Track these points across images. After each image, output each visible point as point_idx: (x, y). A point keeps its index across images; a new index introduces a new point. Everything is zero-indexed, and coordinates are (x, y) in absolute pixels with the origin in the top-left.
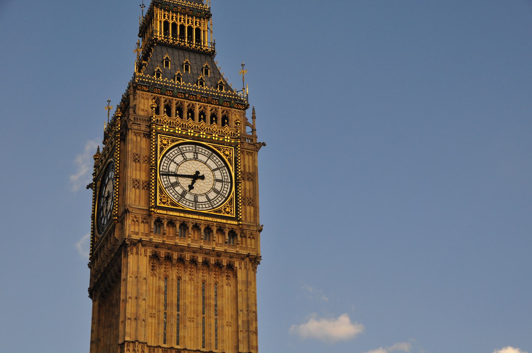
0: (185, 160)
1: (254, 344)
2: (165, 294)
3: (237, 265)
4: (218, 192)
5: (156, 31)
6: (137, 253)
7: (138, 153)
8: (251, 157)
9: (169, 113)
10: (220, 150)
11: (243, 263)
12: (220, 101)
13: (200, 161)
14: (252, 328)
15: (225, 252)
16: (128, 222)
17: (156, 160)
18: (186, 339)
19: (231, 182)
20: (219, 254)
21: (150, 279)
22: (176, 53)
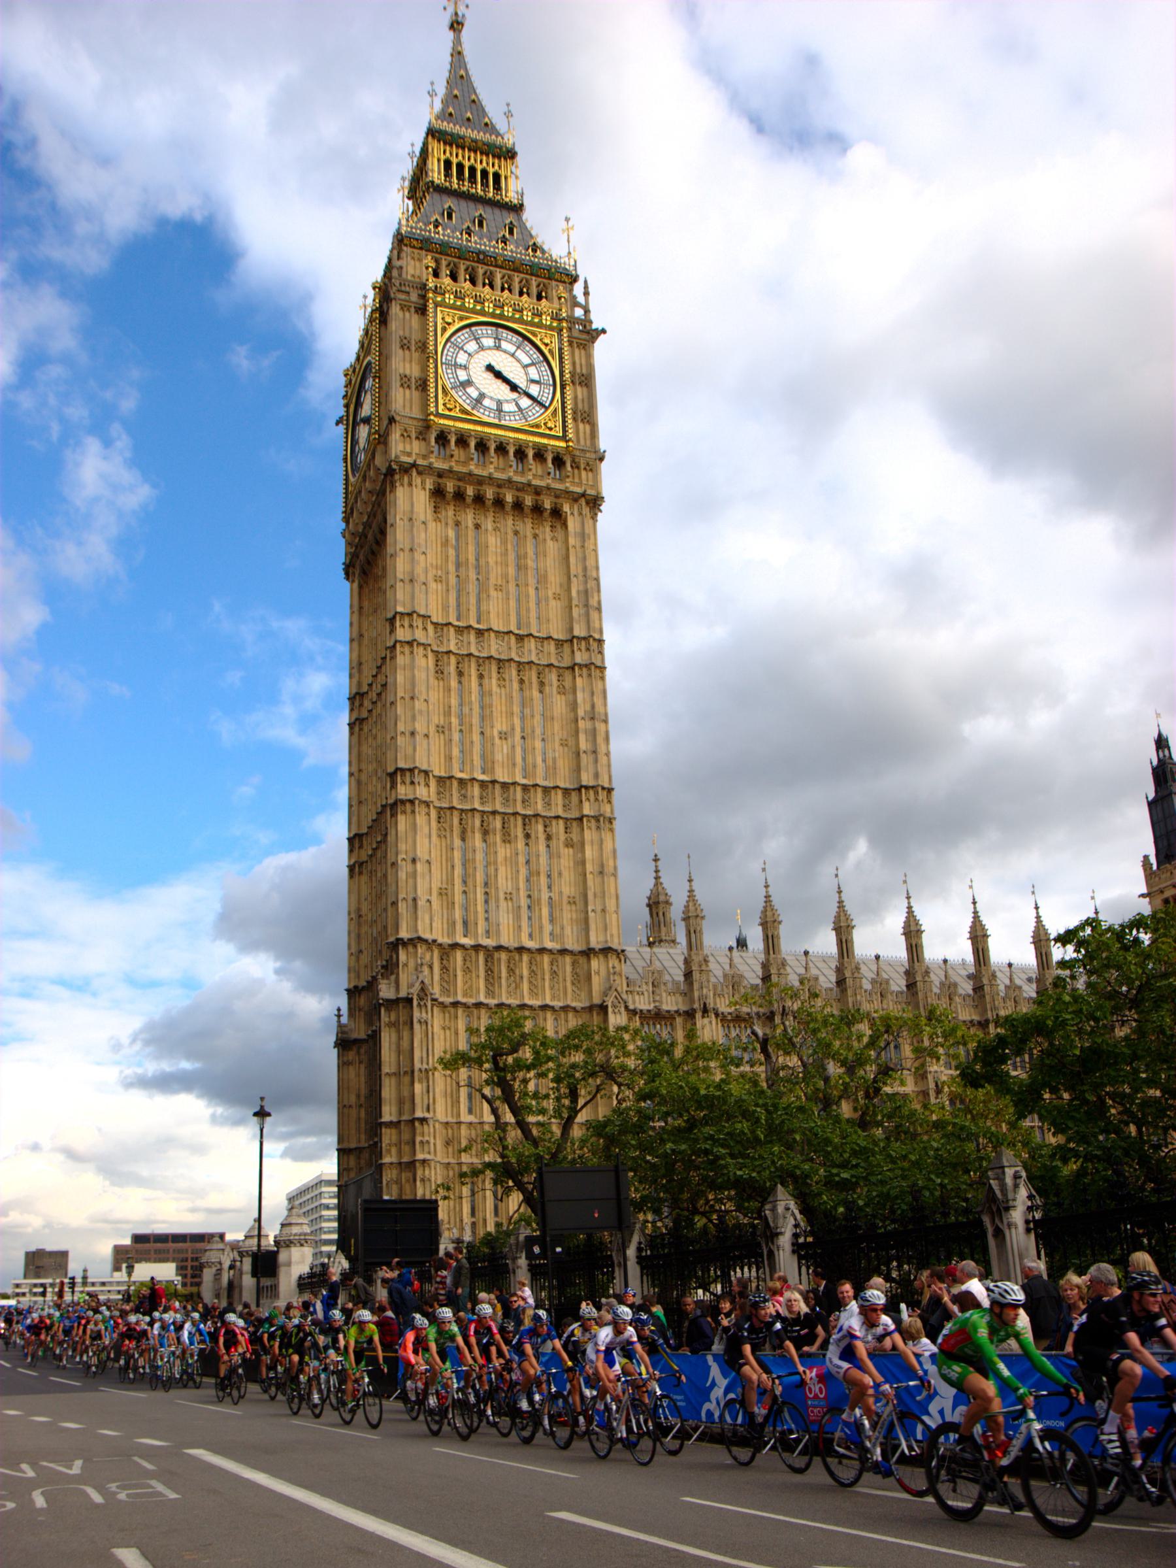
0: (482, 348)
1: (597, 625)
2: (457, 549)
3: (566, 508)
5: (433, 171)
6: (410, 485)
7: (407, 335)
8: (583, 352)
10: (535, 335)
11: (576, 507)
12: (534, 270)
13: (505, 352)
14: (593, 602)
15: (548, 488)
18: (492, 616)
20: (537, 491)
22: (463, 203)
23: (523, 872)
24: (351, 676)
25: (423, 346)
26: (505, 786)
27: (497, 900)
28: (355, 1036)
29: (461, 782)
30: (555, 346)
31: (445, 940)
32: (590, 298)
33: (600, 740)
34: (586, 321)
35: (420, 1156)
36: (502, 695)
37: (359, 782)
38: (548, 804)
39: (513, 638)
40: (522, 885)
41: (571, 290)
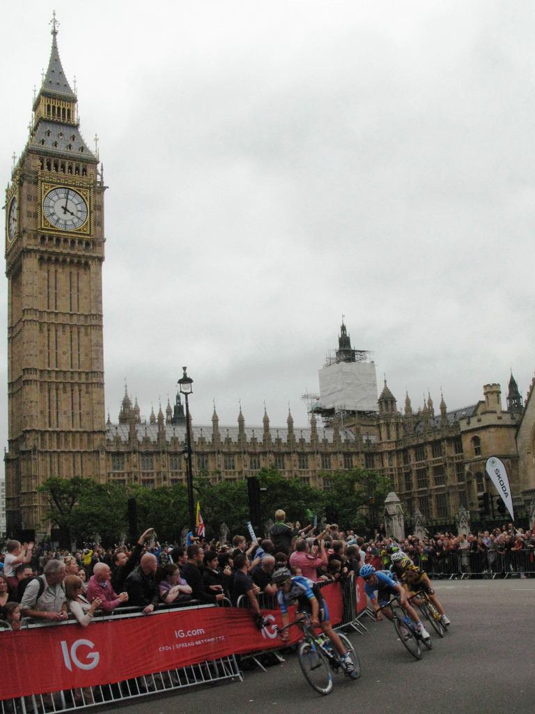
0: (59, 198)
4: (79, 219)
9: (49, 169)
16: (25, 238)
19: (87, 212)
20: (80, 256)
24: (9, 319)
25: (36, 199)
26: (65, 372)
27: (61, 414)
28: (11, 457)
29: (49, 371)
30: (88, 195)
31: (43, 429)
32: (104, 172)
33: (100, 354)
34: (101, 183)
36: (64, 338)
37: (12, 362)
38: (80, 378)
40: (70, 408)
41: (96, 167)
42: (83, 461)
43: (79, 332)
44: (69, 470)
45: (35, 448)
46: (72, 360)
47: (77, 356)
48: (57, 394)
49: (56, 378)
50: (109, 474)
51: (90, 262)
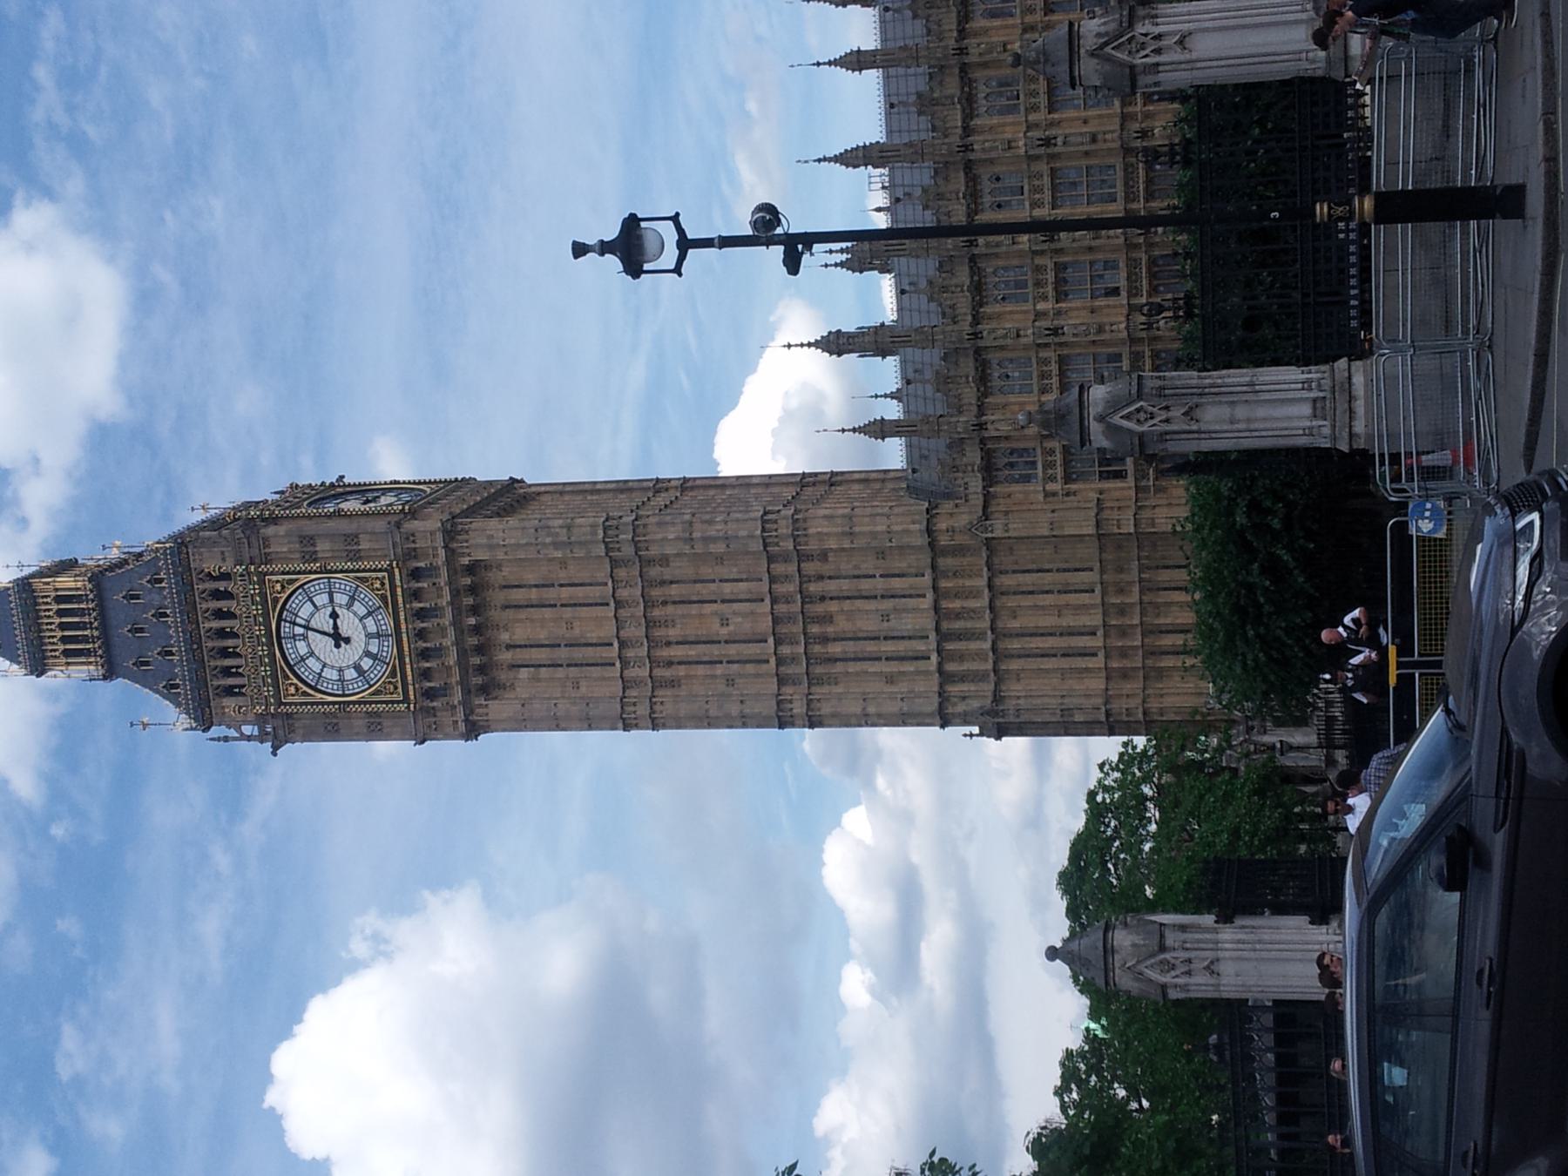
0: (312, 654)
4: (352, 599)
15: (450, 583)
17: (329, 703)
20: (456, 593)
21: (522, 692)
23: (859, 603)
26: (776, 621)
30: (280, 578)
35: (1141, 716)
39: (621, 611)
40: (871, 605)
42: (1016, 567)
43: (663, 583)
44: (1043, 608)
45: (988, 713)
46: (740, 601)
47: (727, 588)
48: (835, 640)
49: (793, 642)
50: (1048, 494)
51: (465, 561)
